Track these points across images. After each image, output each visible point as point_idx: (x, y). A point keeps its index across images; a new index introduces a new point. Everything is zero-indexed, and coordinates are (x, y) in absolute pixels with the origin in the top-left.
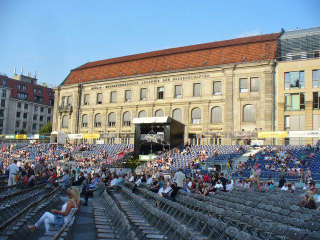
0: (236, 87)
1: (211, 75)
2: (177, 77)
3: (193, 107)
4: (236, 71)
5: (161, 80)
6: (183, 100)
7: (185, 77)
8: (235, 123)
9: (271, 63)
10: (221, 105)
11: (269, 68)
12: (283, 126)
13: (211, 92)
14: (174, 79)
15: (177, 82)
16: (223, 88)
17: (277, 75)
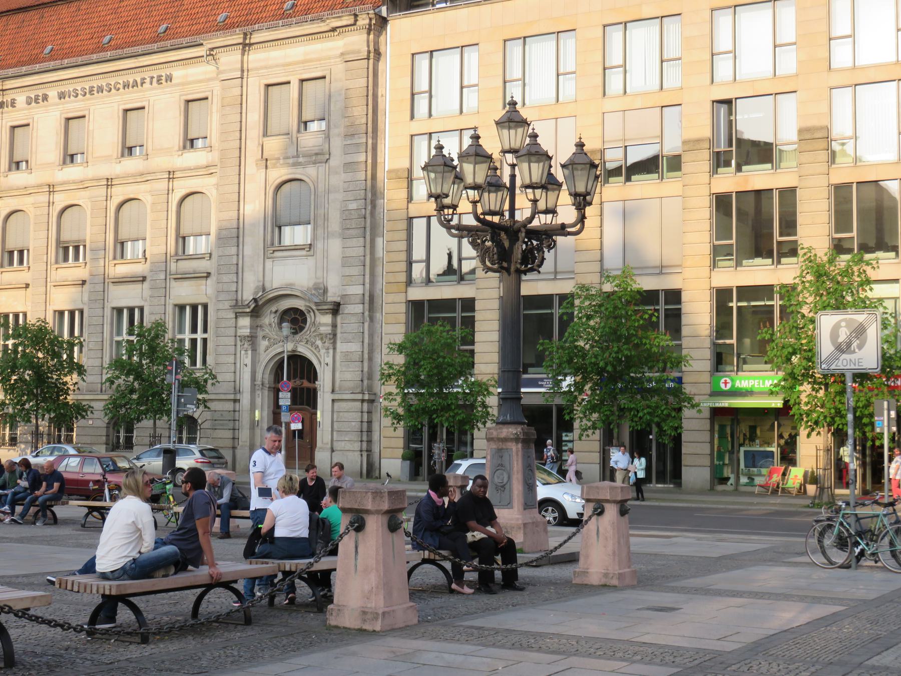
0: (254, 117)
1: (178, 73)
2: (69, 87)
3: (121, 198)
4: (255, 57)
5: (21, 99)
6: (90, 172)
7: (95, 83)
8: (248, 250)
9: (363, 21)
10: (205, 184)
11: (357, 41)
12: (403, 256)
13: (176, 139)
14: (62, 96)
15: (73, 107)
16: (212, 122)
17: (387, 66)
